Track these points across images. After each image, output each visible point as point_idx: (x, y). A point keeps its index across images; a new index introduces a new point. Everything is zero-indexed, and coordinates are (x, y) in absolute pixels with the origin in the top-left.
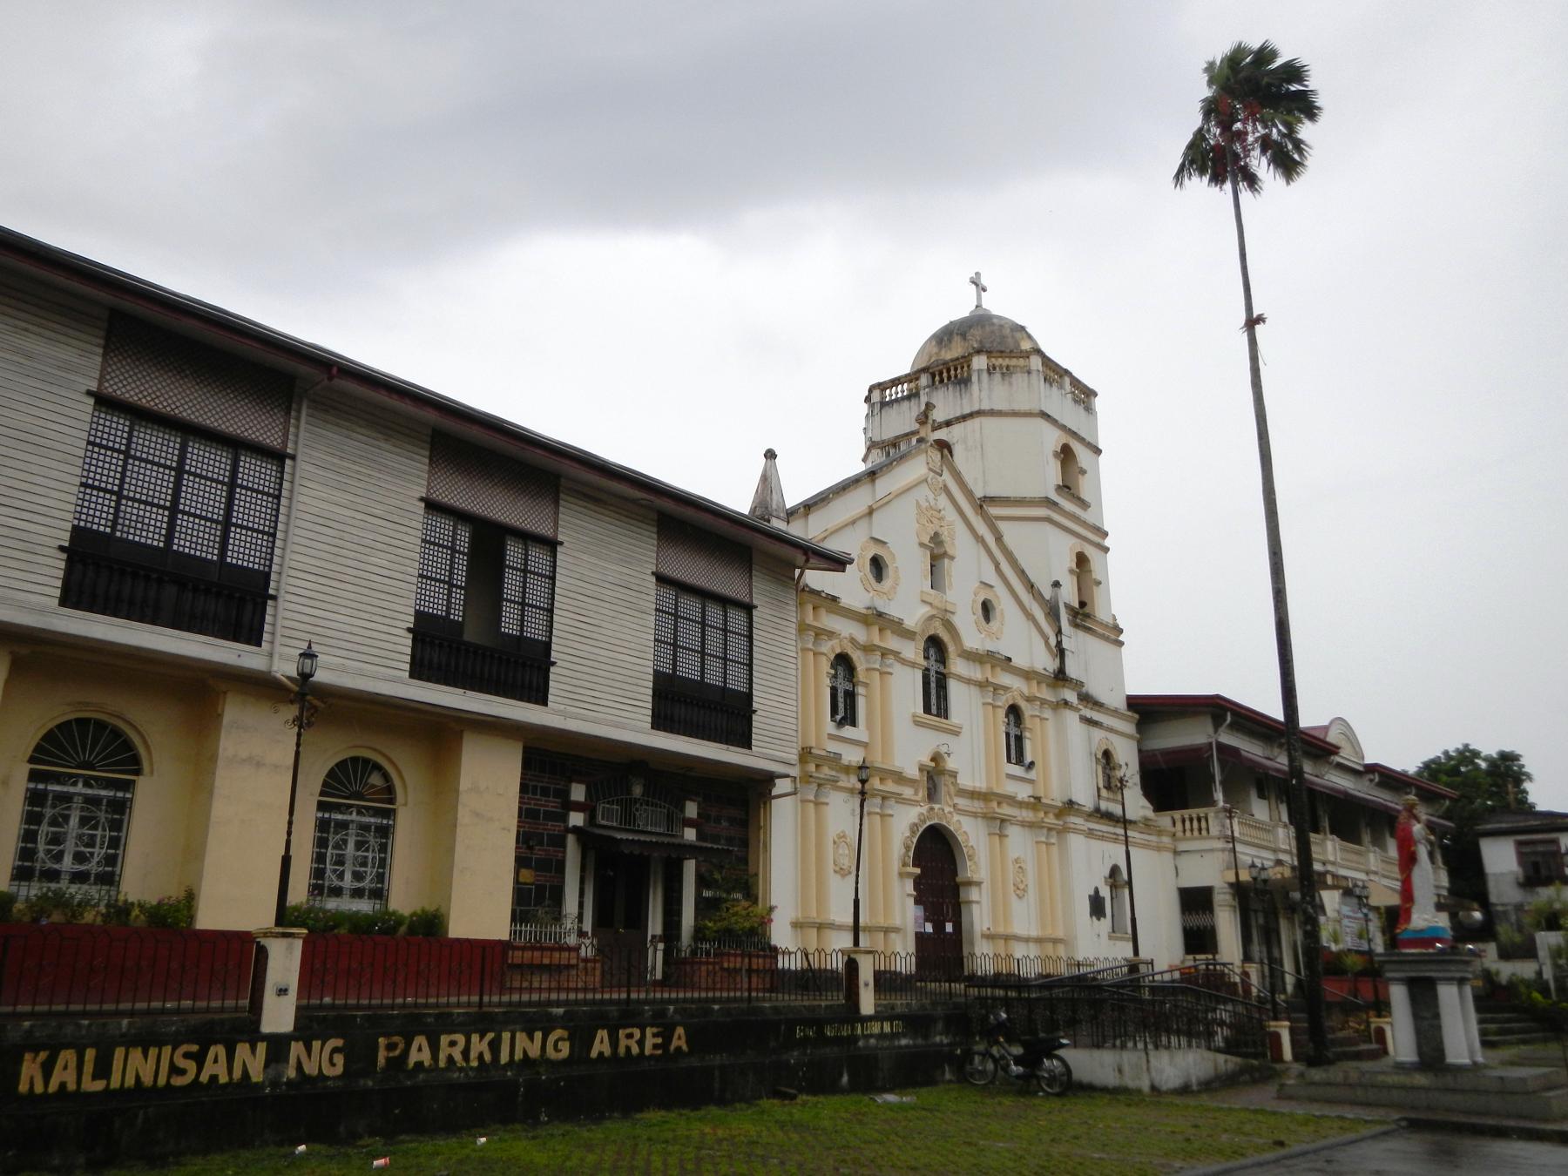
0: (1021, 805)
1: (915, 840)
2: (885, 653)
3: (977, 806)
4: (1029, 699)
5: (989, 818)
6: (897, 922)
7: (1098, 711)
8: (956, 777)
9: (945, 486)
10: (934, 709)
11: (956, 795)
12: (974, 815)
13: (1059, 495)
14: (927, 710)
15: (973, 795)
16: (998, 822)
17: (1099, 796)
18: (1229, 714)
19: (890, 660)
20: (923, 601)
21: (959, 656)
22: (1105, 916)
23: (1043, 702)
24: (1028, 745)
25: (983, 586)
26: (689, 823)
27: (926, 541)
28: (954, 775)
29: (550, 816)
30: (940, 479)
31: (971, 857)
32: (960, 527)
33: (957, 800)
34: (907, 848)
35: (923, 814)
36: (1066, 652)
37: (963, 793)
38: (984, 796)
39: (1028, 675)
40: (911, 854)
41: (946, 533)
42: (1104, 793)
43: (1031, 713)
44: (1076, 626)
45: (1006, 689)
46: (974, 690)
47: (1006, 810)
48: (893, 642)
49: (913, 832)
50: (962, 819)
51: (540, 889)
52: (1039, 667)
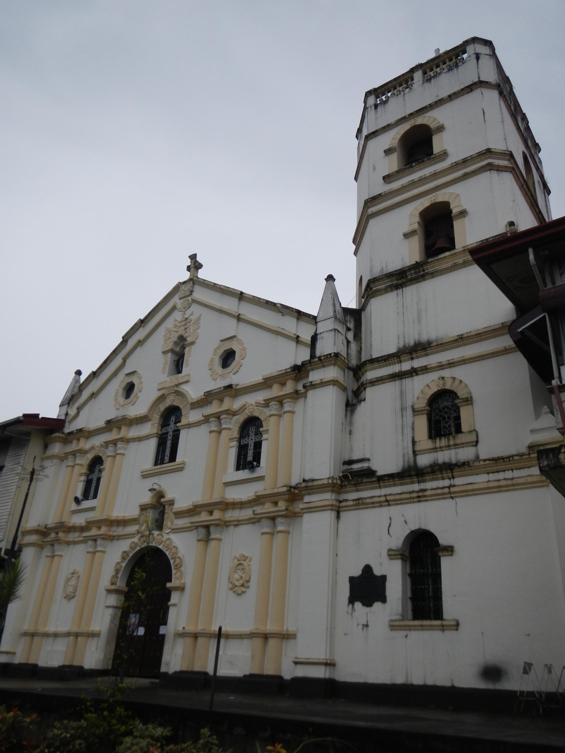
1: (124, 565)
2: (114, 443)
4: (267, 403)
5: (195, 527)
6: (95, 627)
7: (427, 355)
8: (173, 504)
9: (192, 299)
10: (167, 459)
11: (176, 518)
13: (389, 183)
14: (159, 460)
16: (202, 531)
17: (414, 452)
18: (531, 251)
19: (120, 445)
20: (159, 390)
21: (192, 409)
22: (383, 600)
23: (280, 401)
24: (265, 446)
25: (222, 343)
27: (170, 346)
30: (189, 298)
31: (179, 566)
32: (207, 314)
34: (117, 571)
35: (134, 542)
36: (319, 336)
37: (179, 514)
39: (267, 383)
40: (119, 575)
41: (191, 330)
43: (268, 414)
45: (232, 413)
46: (204, 429)
48: (125, 432)
49: (123, 558)
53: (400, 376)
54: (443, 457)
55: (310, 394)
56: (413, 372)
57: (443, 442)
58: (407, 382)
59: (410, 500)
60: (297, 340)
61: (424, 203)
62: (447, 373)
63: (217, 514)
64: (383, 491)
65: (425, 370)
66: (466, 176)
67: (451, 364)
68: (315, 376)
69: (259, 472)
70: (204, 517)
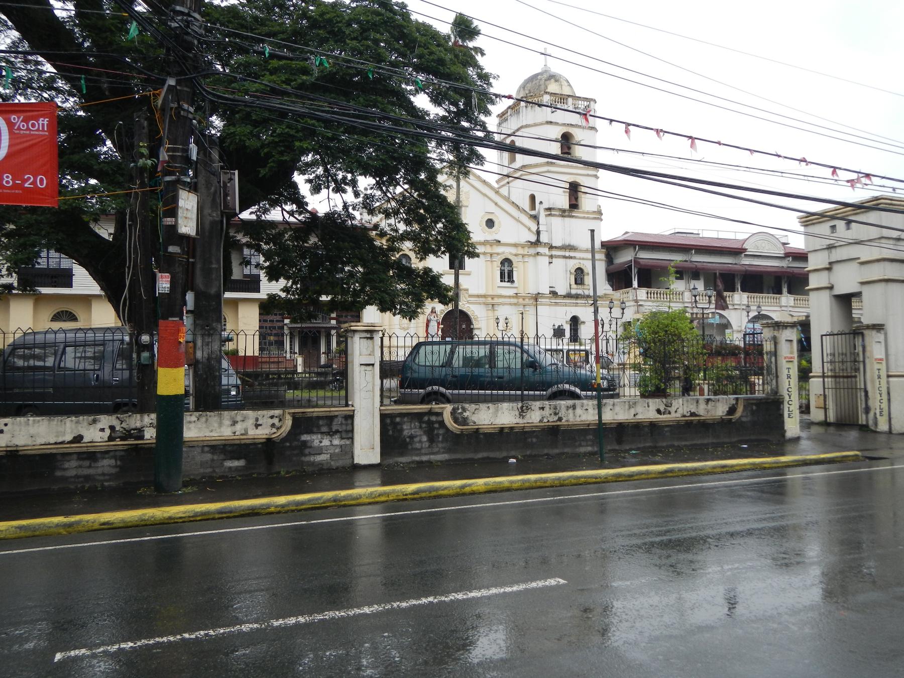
0: (510, 297)
3: (482, 300)
4: (516, 255)
5: (486, 304)
12: (480, 304)
15: (478, 296)
23: (523, 256)
26: (333, 319)
28: (467, 290)
29: (277, 321)
33: (469, 299)
37: (471, 296)
38: (485, 296)
39: (515, 245)
42: (574, 286)
44: (563, 216)
45: (498, 254)
47: (496, 300)
50: (470, 306)
51: (276, 342)
52: (523, 240)
53: (565, 257)
54: (580, 292)
55: (539, 258)
56: (570, 258)
57: (580, 286)
58: (568, 260)
59: (573, 306)
60: (529, 229)
61: (571, 179)
62: (581, 261)
63: (496, 300)
64: (564, 301)
65: (575, 258)
66: (588, 175)
67: (583, 259)
68: (541, 250)
69: (515, 285)
70: (490, 300)
